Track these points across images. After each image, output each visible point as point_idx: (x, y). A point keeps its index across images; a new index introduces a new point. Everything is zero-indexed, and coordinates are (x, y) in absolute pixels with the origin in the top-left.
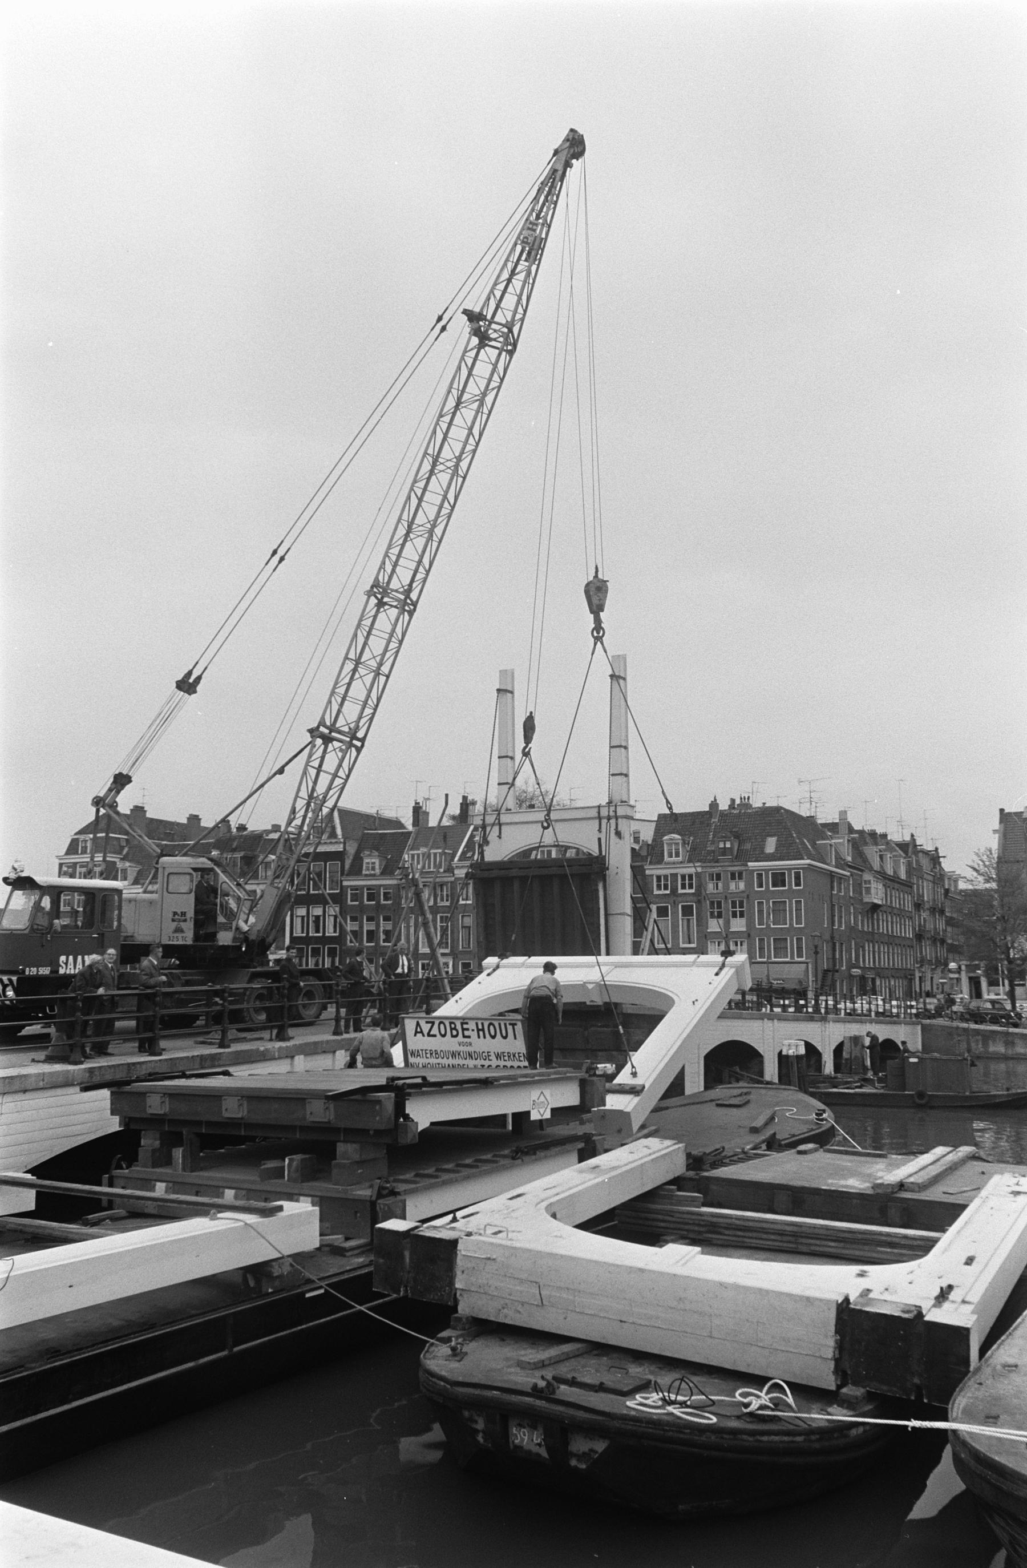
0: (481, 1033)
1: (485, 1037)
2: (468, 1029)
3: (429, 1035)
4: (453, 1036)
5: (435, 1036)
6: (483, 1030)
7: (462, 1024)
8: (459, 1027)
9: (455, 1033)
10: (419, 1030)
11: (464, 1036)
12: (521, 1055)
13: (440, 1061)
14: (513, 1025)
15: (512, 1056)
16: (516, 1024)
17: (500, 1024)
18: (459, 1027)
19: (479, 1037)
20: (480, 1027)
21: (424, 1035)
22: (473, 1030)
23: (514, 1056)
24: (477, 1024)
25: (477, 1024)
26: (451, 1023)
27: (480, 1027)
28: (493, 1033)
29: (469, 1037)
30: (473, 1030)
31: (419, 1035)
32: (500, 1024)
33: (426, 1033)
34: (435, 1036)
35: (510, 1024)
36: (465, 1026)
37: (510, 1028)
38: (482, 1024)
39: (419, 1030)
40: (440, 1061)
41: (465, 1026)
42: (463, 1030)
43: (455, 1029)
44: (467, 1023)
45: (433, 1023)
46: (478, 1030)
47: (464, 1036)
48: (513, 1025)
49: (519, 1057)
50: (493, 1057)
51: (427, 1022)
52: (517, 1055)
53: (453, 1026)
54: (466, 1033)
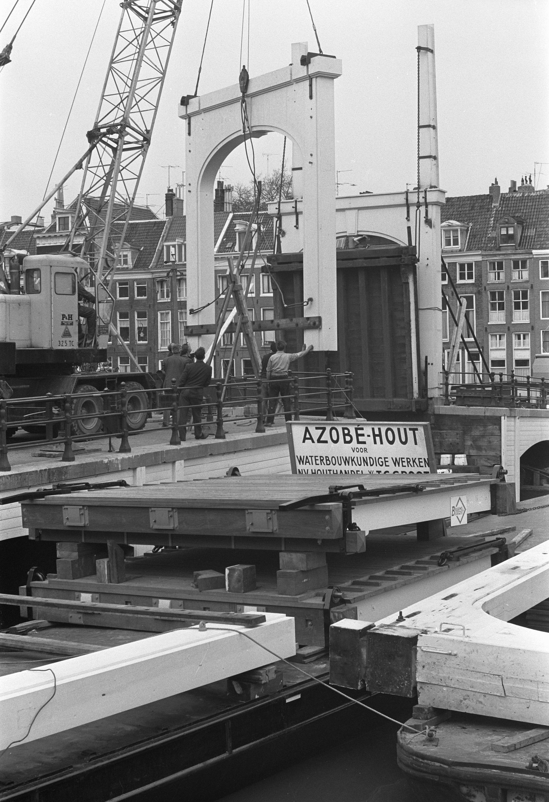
0: (378, 438)
1: (382, 443)
2: (363, 435)
3: (319, 441)
4: (346, 442)
5: (326, 442)
6: (380, 435)
7: (356, 429)
8: (353, 433)
9: (348, 438)
10: (308, 436)
11: (359, 442)
12: (423, 460)
13: (331, 467)
14: (414, 430)
15: (411, 462)
16: (417, 429)
17: (399, 430)
18: (353, 433)
19: (375, 443)
20: (377, 432)
21: (313, 442)
22: (369, 436)
23: (414, 461)
24: (373, 429)
25: (373, 429)
26: (344, 429)
27: (377, 432)
28: (391, 439)
29: (364, 443)
30: (369, 436)
31: (308, 442)
32: (399, 430)
33: (316, 441)
34: (326, 442)
35: (410, 429)
36: (360, 432)
37: (410, 434)
38: (379, 429)
39: (308, 436)
40: (331, 467)
41: (360, 432)
42: (358, 435)
43: (348, 434)
44: (362, 429)
45: (324, 429)
46: (375, 436)
47: (359, 442)
48: (414, 430)
49: (420, 462)
50: (390, 463)
51: (317, 428)
52: (417, 461)
53: (346, 432)
54: (361, 439)
